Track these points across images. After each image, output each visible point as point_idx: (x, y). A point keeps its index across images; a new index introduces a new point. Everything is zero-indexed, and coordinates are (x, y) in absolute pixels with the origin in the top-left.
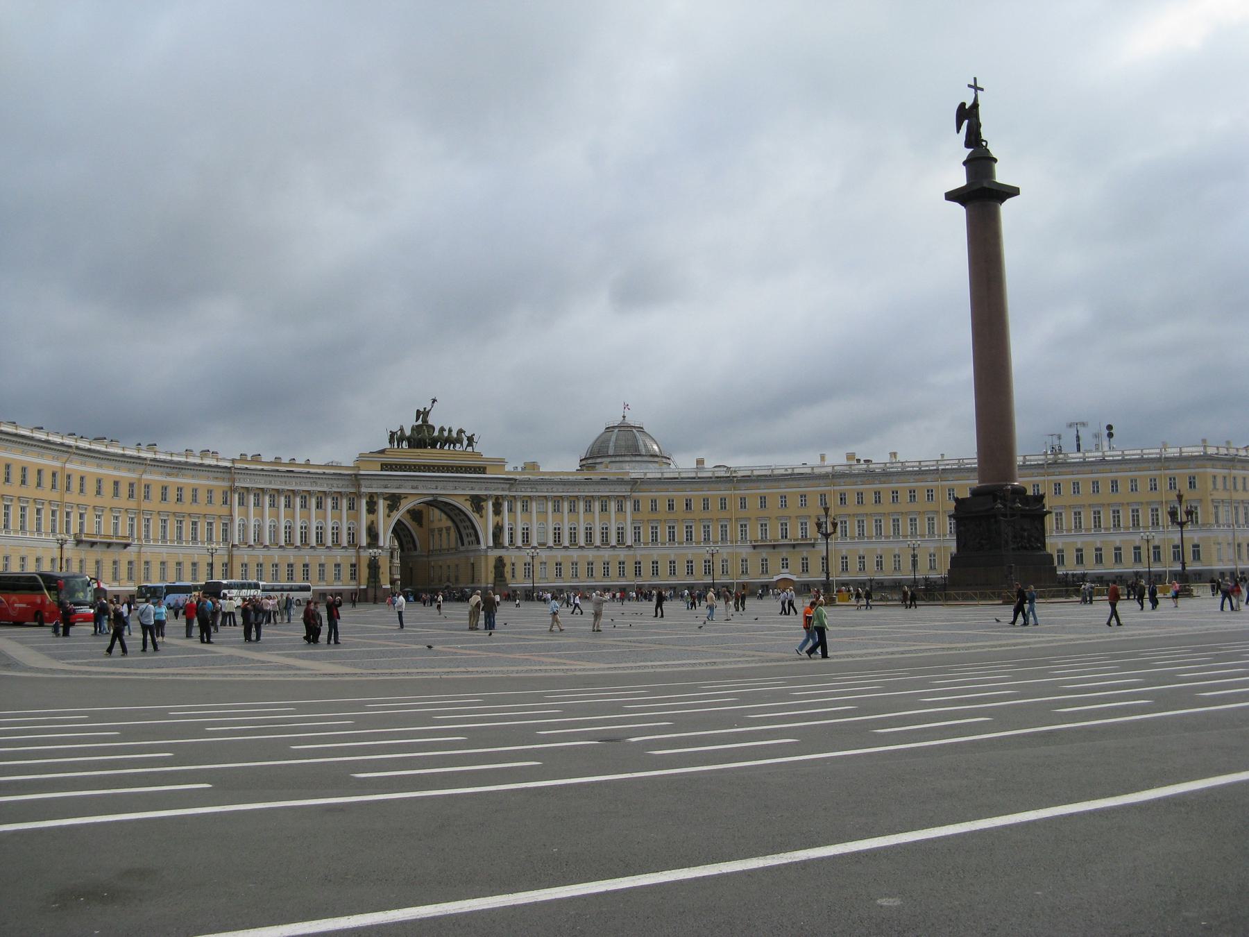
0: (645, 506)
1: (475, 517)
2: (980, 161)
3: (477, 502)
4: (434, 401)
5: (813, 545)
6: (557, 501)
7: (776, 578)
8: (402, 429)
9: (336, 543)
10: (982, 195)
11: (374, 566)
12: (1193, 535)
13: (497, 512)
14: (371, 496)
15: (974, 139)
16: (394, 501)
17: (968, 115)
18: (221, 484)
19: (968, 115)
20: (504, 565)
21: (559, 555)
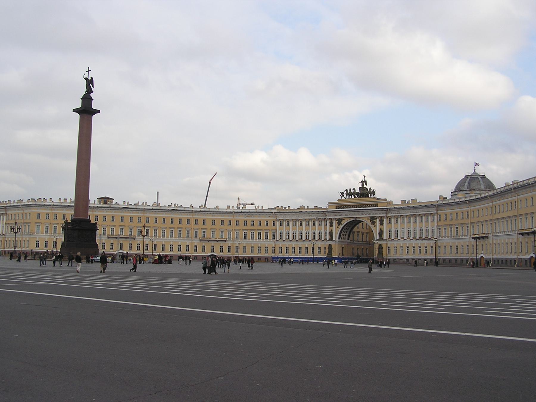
0: (443, 217)
1: (372, 226)
2: (87, 99)
3: (373, 220)
4: (365, 176)
5: (487, 237)
6: (409, 217)
7: (480, 256)
8: (346, 190)
9: (320, 238)
10: (86, 111)
11: (330, 247)
12: (19, 237)
13: (381, 224)
14: (331, 219)
15: (89, 91)
16: (340, 221)
17: (90, 82)
18: (271, 219)
19: (90, 82)
20: (382, 248)
21: (408, 243)
